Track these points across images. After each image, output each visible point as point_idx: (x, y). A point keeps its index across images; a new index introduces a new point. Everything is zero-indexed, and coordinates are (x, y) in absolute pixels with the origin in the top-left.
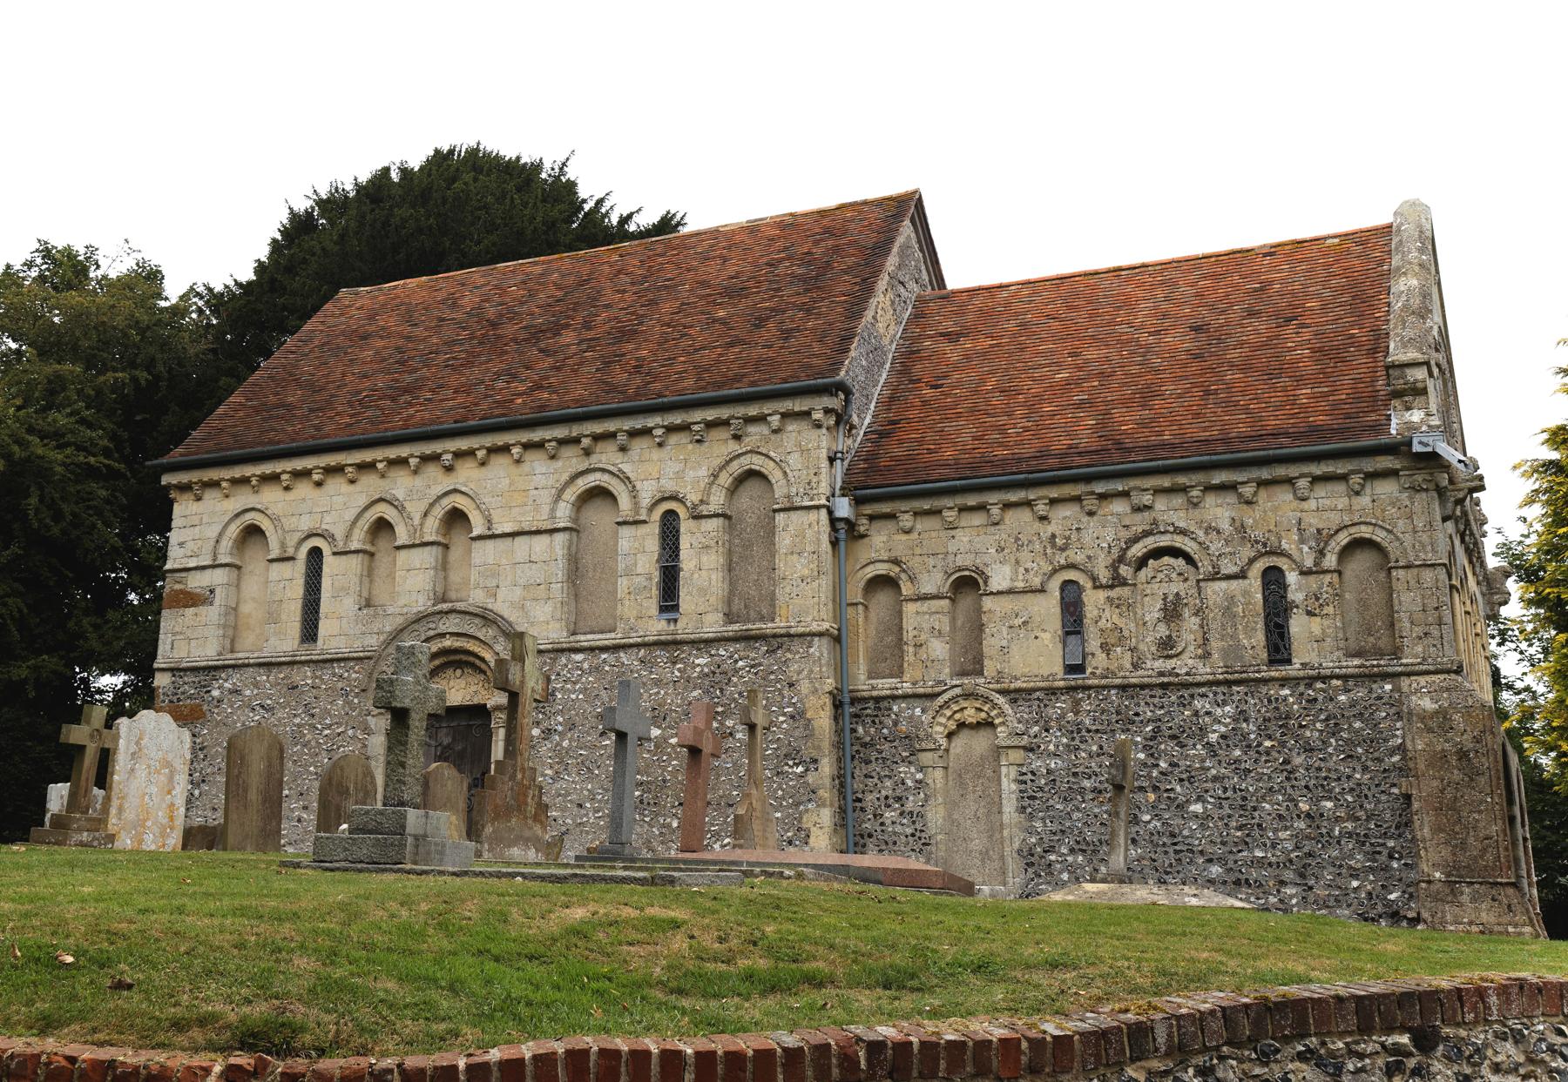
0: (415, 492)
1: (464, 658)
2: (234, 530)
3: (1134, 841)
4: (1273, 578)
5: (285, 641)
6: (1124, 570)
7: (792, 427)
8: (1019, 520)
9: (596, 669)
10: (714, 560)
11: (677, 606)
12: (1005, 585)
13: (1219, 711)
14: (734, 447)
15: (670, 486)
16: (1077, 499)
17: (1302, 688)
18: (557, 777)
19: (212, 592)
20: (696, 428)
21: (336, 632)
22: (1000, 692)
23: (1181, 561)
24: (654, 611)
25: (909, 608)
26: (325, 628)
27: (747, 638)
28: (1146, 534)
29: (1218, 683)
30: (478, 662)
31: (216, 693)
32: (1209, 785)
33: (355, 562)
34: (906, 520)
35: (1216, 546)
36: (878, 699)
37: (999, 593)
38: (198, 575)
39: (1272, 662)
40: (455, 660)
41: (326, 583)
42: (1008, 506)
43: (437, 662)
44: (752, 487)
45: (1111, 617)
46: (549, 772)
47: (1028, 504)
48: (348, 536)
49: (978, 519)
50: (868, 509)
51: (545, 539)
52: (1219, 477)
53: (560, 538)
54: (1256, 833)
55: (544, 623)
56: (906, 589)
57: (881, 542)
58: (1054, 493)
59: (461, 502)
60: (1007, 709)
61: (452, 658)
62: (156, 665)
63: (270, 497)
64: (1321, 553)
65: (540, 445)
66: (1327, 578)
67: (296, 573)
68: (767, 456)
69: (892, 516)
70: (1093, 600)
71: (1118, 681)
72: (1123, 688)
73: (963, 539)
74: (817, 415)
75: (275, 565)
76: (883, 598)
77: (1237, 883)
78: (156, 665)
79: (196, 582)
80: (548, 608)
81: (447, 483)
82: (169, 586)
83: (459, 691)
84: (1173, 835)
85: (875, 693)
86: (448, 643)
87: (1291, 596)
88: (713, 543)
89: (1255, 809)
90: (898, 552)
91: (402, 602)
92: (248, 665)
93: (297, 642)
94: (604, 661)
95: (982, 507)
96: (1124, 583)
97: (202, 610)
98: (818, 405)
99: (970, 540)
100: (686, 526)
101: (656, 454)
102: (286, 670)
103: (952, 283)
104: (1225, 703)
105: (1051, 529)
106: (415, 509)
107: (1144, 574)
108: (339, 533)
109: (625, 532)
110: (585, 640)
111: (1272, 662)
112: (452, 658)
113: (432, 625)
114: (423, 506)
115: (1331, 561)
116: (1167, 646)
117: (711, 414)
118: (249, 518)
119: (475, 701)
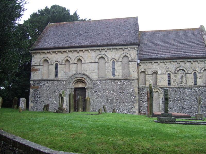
0: (73, 56)
2: (43, 60)
3: (177, 107)
4: (195, 73)
5: (52, 77)
6: (176, 72)
7: (132, 50)
8: (162, 64)
9: (102, 83)
10: (120, 68)
11: (115, 74)
12: (160, 73)
13: (188, 91)
14: (123, 52)
15: (113, 57)
16: (170, 62)
17: (198, 88)
18: (97, 98)
19: (39, 69)
20: (118, 49)
21: (60, 76)
22: (160, 88)
23: (183, 71)
24: (111, 75)
25: (147, 76)
26: (59, 75)
27: (126, 79)
28: (179, 67)
29: (188, 87)
30: (83, 81)
31: (41, 84)
32: (187, 100)
33: (63, 66)
34: (147, 64)
35: (188, 69)
36: (142, 88)
37: (160, 74)
38: (37, 66)
39: (195, 84)
41: (59, 69)
42: (160, 62)
43: (77, 81)
44: (126, 58)
45: (175, 78)
46: (96, 97)
47: (163, 62)
48: (62, 62)
49: (156, 64)
50: (142, 62)
51: (94, 64)
52: (189, 60)
53: (96, 64)
54: (192, 106)
55: (94, 76)
56: (146, 73)
57: (143, 67)
58: (167, 61)
59: (80, 58)
60: (161, 90)
62: (31, 80)
63: (48, 55)
64: (201, 71)
65: (93, 50)
66: (202, 74)
67: (54, 67)
68: (128, 54)
69: (145, 63)
70: (172, 76)
71: (175, 87)
72: (176, 87)
73: (154, 66)
74: (135, 48)
75: (50, 66)
76: (143, 74)
77: (190, 113)
78: (31, 80)
79: (36, 68)
80: (95, 74)
81: (78, 55)
82: (32, 68)
83: (80, 85)
84: (182, 107)
85: (142, 87)
86: (79, 78)
87: (197, 76)
88: (120, 66)
89: (192, 103)
90: (145, 68)
91: (71, 72)
92: (46, 80)
93: (54, 77)
94: (104, 82)
95: (157, 62)
96: (176, 74)
97: (38, 72)
98: (136, 47)
99: (155, 66)
100: (116, 63)
101: (111, 52)
102: (53, 81)
103: (140, 31)
104: (189, 90)
105: (167, 66)
106: (73, 58)
107: (178, 73)
108: (60, 61)
109: (106, 63)
110: (101, 79)
111: (195, 84)
114: (74, 58)
115: (202, 72)
116: (181, 82)
117: (120, 47)
118: (45, 58)
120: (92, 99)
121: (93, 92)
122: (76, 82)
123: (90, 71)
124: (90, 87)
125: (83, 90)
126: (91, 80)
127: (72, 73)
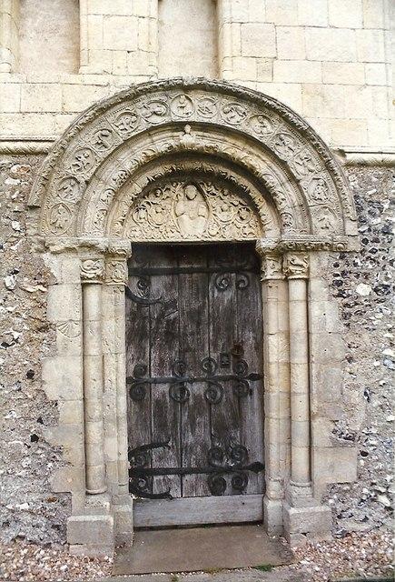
1: (208, 166)
40: (191, 170)
43: (160, 171)
61: (188, 165)
83: (195, 219)
86: (190, 139)
91: (98, 67)
112: (188, 165)
120: (355, 366)
121: (363, 290)
123: (313, 75)
124: (322, 236)
125: (239, 260)
126: (328, 167)
127: (102, 80)
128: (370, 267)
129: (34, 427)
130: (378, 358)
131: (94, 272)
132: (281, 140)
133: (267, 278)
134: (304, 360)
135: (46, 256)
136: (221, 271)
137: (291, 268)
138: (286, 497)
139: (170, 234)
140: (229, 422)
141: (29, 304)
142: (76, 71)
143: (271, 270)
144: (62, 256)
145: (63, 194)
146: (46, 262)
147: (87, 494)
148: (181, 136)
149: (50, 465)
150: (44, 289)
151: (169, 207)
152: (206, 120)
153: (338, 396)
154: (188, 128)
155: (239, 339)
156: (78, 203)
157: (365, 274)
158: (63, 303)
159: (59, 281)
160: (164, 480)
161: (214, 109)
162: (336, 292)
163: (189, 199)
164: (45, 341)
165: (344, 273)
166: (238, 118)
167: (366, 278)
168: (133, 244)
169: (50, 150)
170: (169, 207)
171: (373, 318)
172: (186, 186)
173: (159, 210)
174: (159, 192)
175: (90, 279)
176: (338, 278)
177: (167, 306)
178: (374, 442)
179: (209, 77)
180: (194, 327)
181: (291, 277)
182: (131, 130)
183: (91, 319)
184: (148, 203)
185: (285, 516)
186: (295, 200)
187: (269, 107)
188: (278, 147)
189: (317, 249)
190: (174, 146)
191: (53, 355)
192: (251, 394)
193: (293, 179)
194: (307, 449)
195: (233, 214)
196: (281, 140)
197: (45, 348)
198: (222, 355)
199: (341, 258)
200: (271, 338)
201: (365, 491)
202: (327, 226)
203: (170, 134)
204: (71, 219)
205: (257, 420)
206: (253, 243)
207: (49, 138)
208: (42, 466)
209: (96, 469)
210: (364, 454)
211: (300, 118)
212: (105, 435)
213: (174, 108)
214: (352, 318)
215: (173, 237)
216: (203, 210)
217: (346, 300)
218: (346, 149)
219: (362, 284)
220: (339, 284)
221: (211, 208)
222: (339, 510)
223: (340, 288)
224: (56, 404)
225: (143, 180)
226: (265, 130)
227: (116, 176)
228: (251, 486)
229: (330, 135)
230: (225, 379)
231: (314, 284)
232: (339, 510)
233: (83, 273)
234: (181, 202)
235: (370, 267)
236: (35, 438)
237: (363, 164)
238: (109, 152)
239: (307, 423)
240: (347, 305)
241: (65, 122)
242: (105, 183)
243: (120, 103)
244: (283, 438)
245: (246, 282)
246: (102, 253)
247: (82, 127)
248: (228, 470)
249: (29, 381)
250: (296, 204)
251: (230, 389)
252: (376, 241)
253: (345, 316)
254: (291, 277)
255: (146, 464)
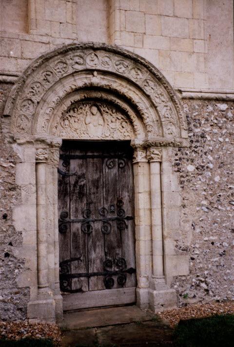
1: (105, 96)
40: (96, 98)
43: (77, 97)
46: (205, 202)
83: (97, 127)
86: (97, 80)
91: (43, 31)
113: (77, 59)
119: (118, 136)
120: (186, 210)
121: (191, 168)
122: (74, 106)
124: (169, 138)
125: (121, 152)
126: (172, 99)
127: (45, 39)
128: (194, 155)
129: (7, 248)
130: (199, 205)
131: (42, 156)
132: (147, 83)
133: (139, 161)
134: (160, 207)
135: (14, 146)
136: (110, 157)
137: (152, 155)
138: (152, 286)
139: (83, 135)
140: (115, 244)
141: (4, 174)
142: (27, 30)
143: (140, 156)
144: (24, 146)
145: (24, 109)
146: (15, 149)
147: (39, 288)
148: (92, 78)
149: (16, 271)
150: (13, 165)
151: (82, 119)
152: (106, 69)
153: (178, 226)
154: (95, 73)
155: (119, 196)
156: (33, 115)
157: (191, 159)
158: (24, 174)
159: (23, 161)
160: (78, 281)
161: (110, 63)
162: (176, 169)
163: (93, 114)
164: (14, 196)
165: (180, 159)
166: (124, 69)
167: (192, 162)
168: (64, 141)
169: (16, 82)
170: (82, 119)
171: (196, 184)
172: (92, 106)
173: (76, 120)
174: (76, 110)
175: (41, 160)
176: (178, 162)
177: (79, 177)
178: (198, 252)
179: (107, 44)
180: (95, 190)
181: (152, 161)
182: (63, 73)
183: (41, 183)
184: (70, 116)
185: (151, 295)
186: (154, 117)
187: (141, 63)
188: (145, 87)
189: (166, 145)
190: (88, 84)
191: (20, 204)
192: (127, 228)
193: (153, 106)
194: (162, 257)
195: (117, 125)
196: (147, 83)
197: (14, 201)
198: (111, 206)
199: (179, 150)
200: (140, 195)
201: (194, 280)
202: (171, 133)
203: (85, 76)
204: (29, 125)
205: (130, 243)
206: (129, 141)
207: (15, 73)
208: (12, 272)
209: (43, 272)
210: (193, 259)
211: (158, 71)
212: (48, 252)
213: (88, 61)
214: (185, 183)
215: (85, 137)
216: (101, 122)
217: (181, 174)
218: (182, 89)
219: (190, 165)
220: (177, 165)
221: (105, 120)
222: (180, 291)
223: (179, 167)
224: (21, 234)
225: (68, 103)
226: (138, 77)
227: (54, 100)
228: (129, 281)
229: (175, 81)
230: (113, 220)
231: (165, 165)
232: (180, 291)
233: (37, 157)
234: (88, 116)
235: (194, 155)
236: (7, 255)
237: (192, 98)
238: (51, 85)
239: (162, 242)
240: (182, 176)
241: (24, 64)
242: (48, 104)
243: (56, 55)
244: (148, 250)
245: (124, 164)
246: (48, 145)
247: (35, 69)
248: (115, 273)
249: (4, 220)
250: (155, 120)
251: (115, 225)
252: (197, 141)
253: (181, 182)
254: (152, 161)
255: (68, 271)
